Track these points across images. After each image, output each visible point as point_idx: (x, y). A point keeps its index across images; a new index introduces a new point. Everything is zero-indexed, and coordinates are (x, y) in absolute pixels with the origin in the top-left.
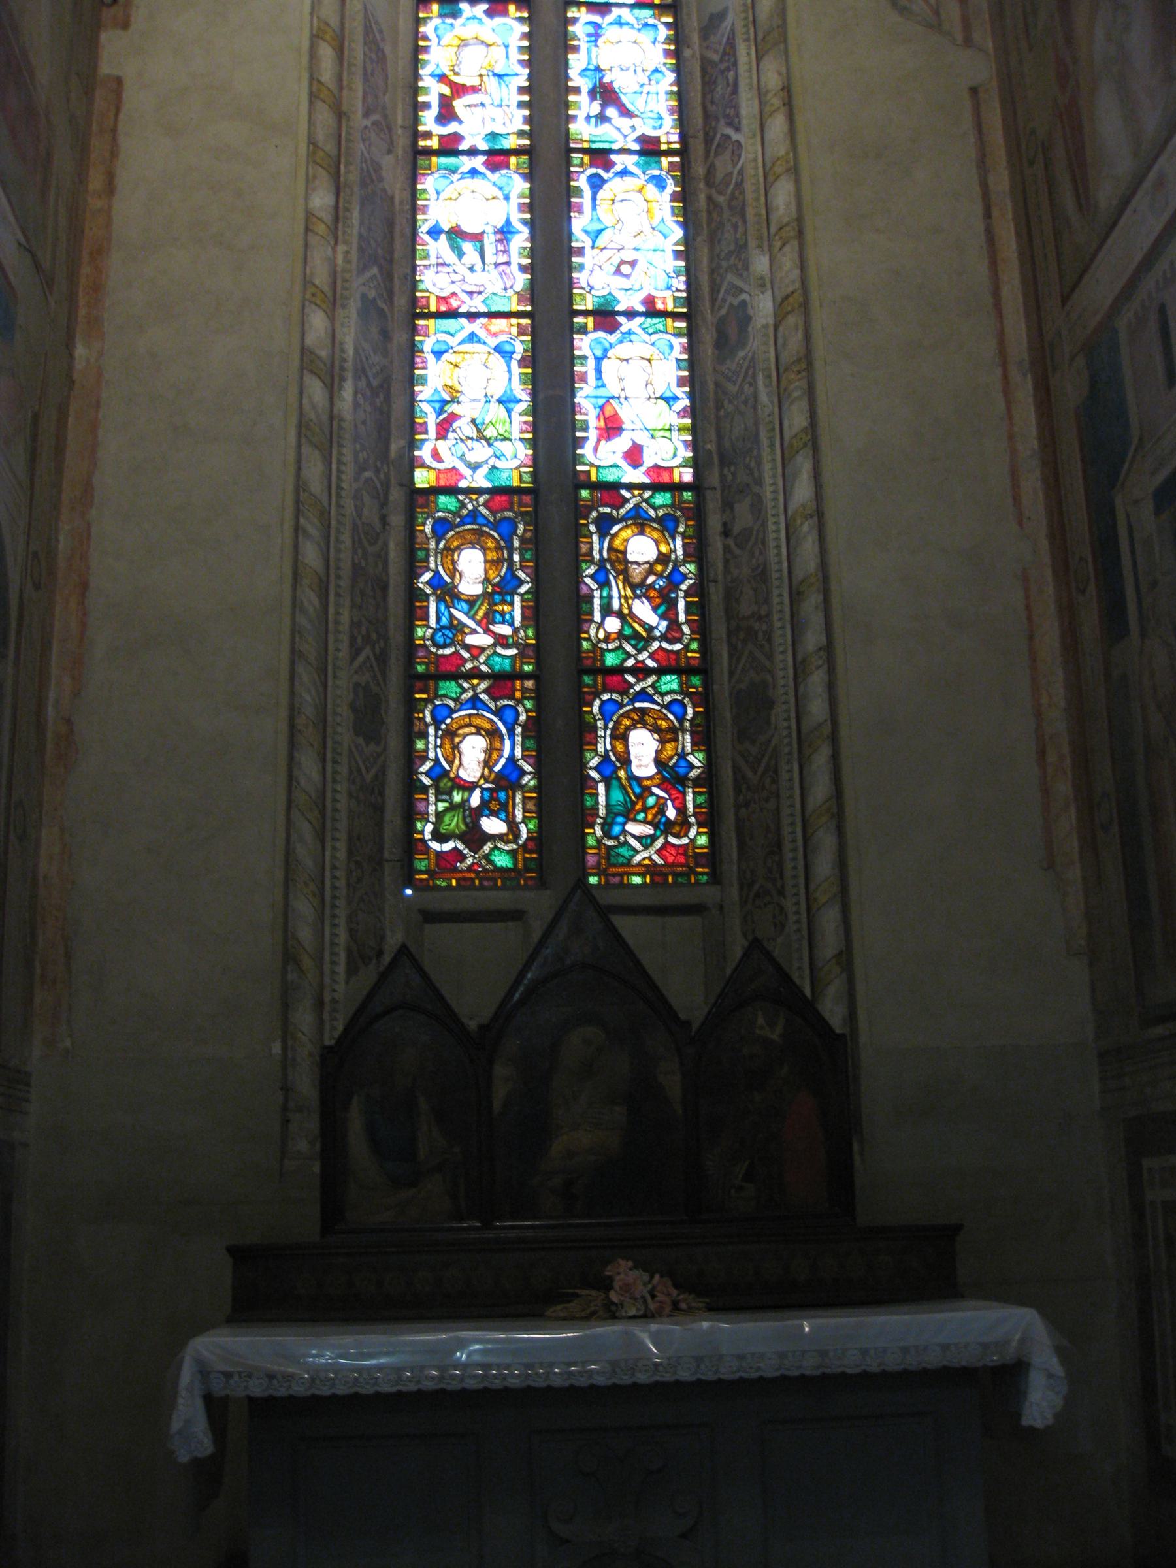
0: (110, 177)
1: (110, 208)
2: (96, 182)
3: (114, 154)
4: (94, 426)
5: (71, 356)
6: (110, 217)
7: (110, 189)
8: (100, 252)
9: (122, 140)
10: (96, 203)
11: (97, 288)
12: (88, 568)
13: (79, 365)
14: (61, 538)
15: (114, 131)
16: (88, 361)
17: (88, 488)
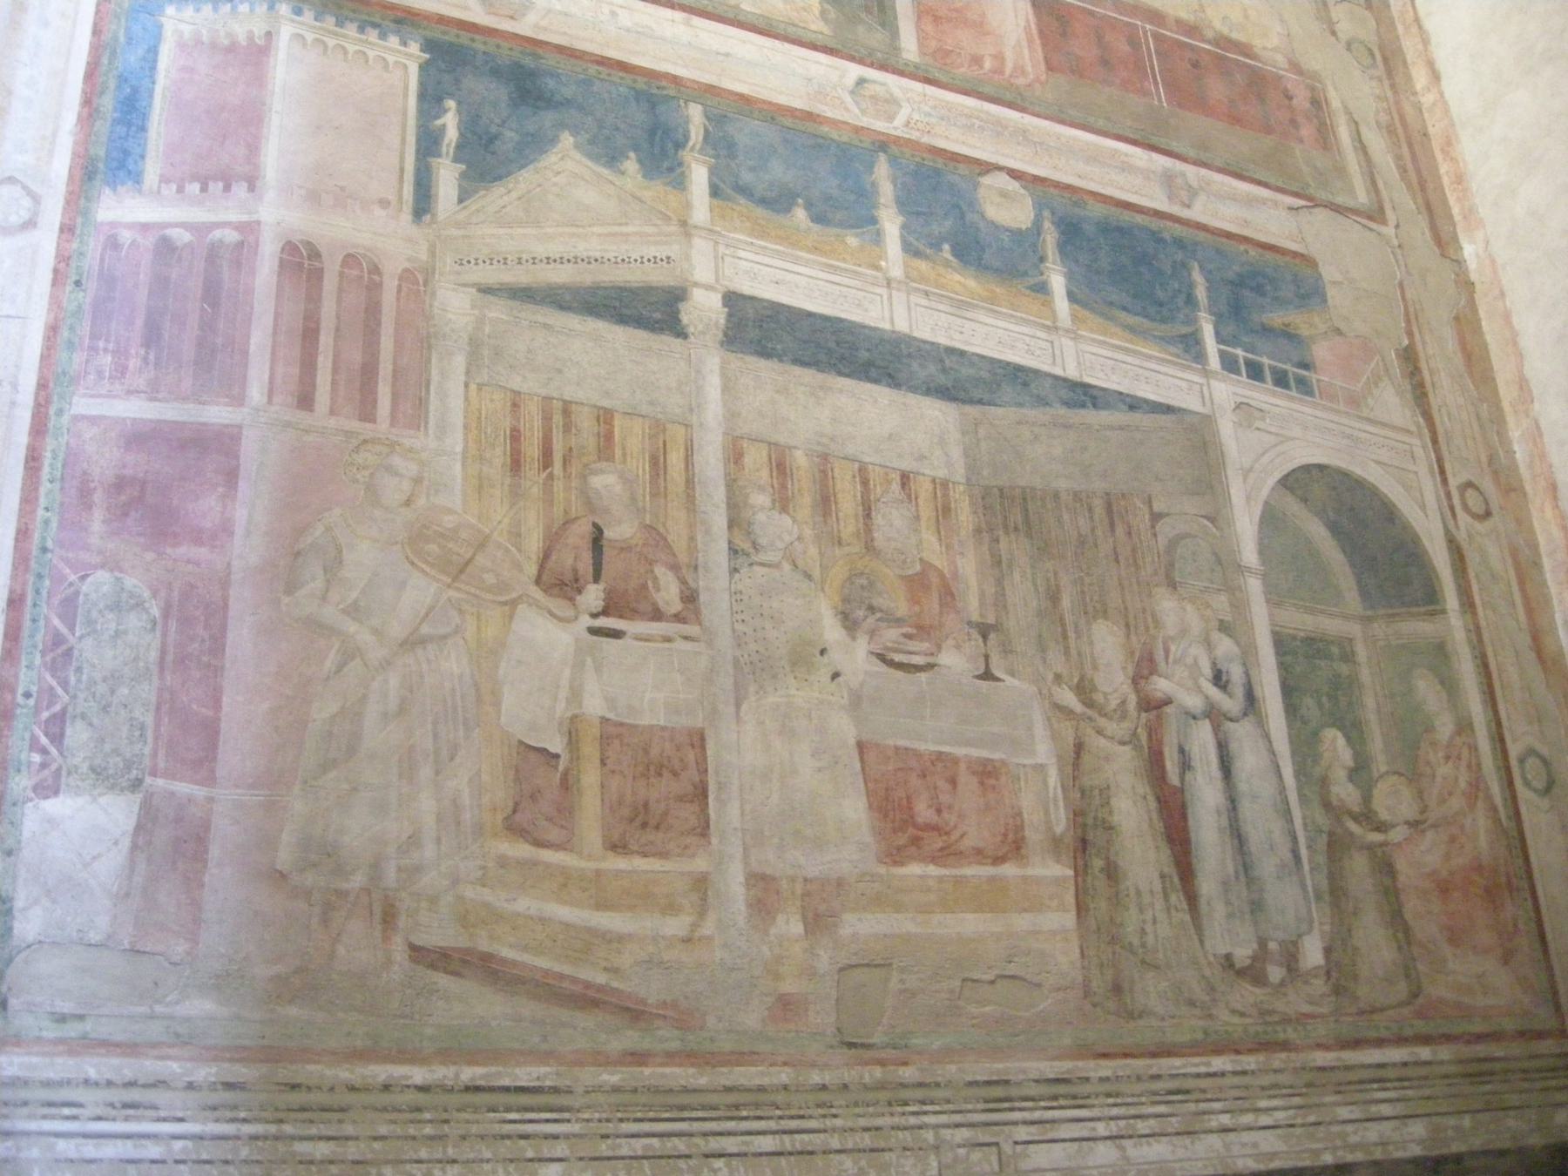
0: (1431, 65)
1: (1442, 94)
2: (1420, 78)
3: (1426, 42)
4: (1507, 317)
5: (1459, 263)
6: (1445, 103)
7: (1436, 77)
8: (1449, 142)
9: (1428, 24)
10: (1427, 99)
11: (1459, 179)
12: (1551, 466)
13: (1472, 265)
14: (1516, 447)
15: (1417, 20)
16: (1477, 256)
17: (1523, 384)
